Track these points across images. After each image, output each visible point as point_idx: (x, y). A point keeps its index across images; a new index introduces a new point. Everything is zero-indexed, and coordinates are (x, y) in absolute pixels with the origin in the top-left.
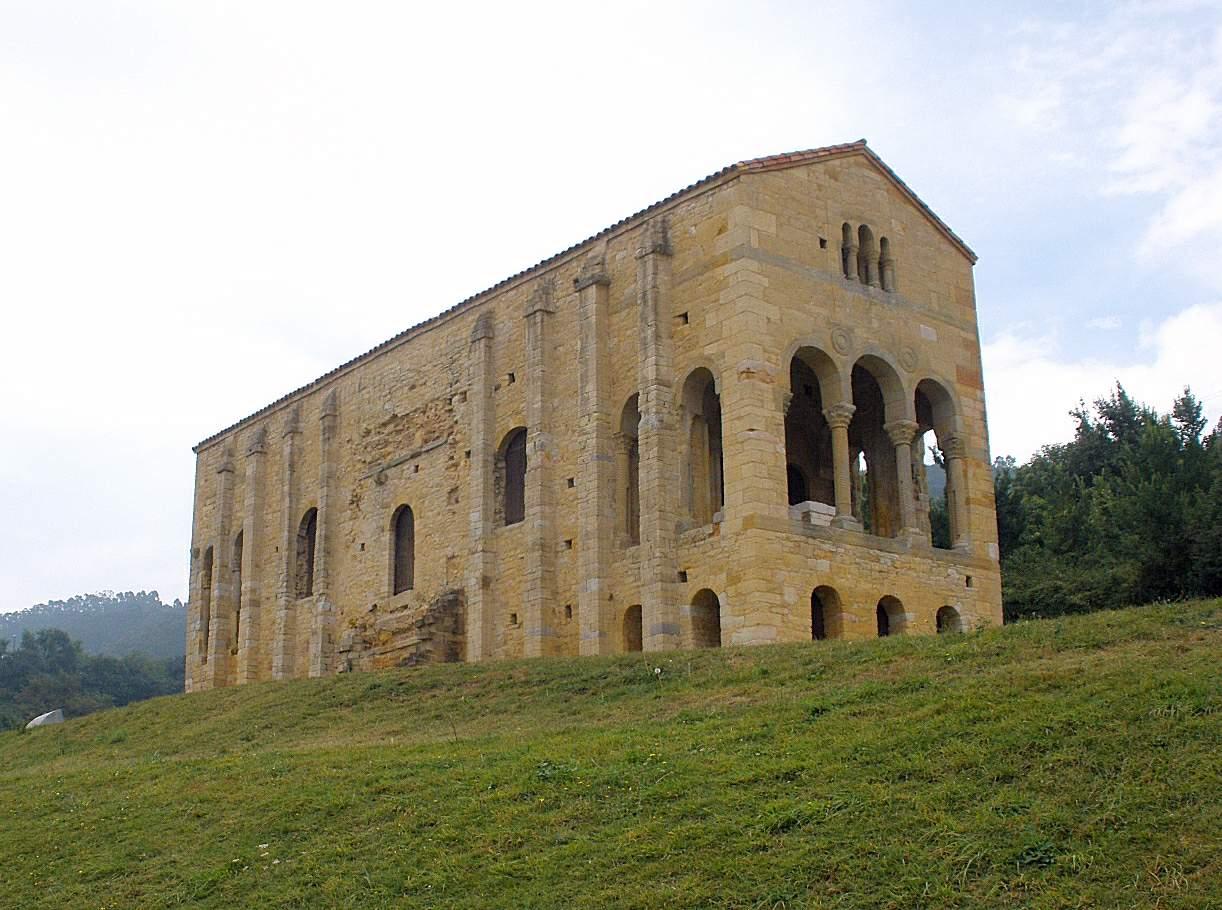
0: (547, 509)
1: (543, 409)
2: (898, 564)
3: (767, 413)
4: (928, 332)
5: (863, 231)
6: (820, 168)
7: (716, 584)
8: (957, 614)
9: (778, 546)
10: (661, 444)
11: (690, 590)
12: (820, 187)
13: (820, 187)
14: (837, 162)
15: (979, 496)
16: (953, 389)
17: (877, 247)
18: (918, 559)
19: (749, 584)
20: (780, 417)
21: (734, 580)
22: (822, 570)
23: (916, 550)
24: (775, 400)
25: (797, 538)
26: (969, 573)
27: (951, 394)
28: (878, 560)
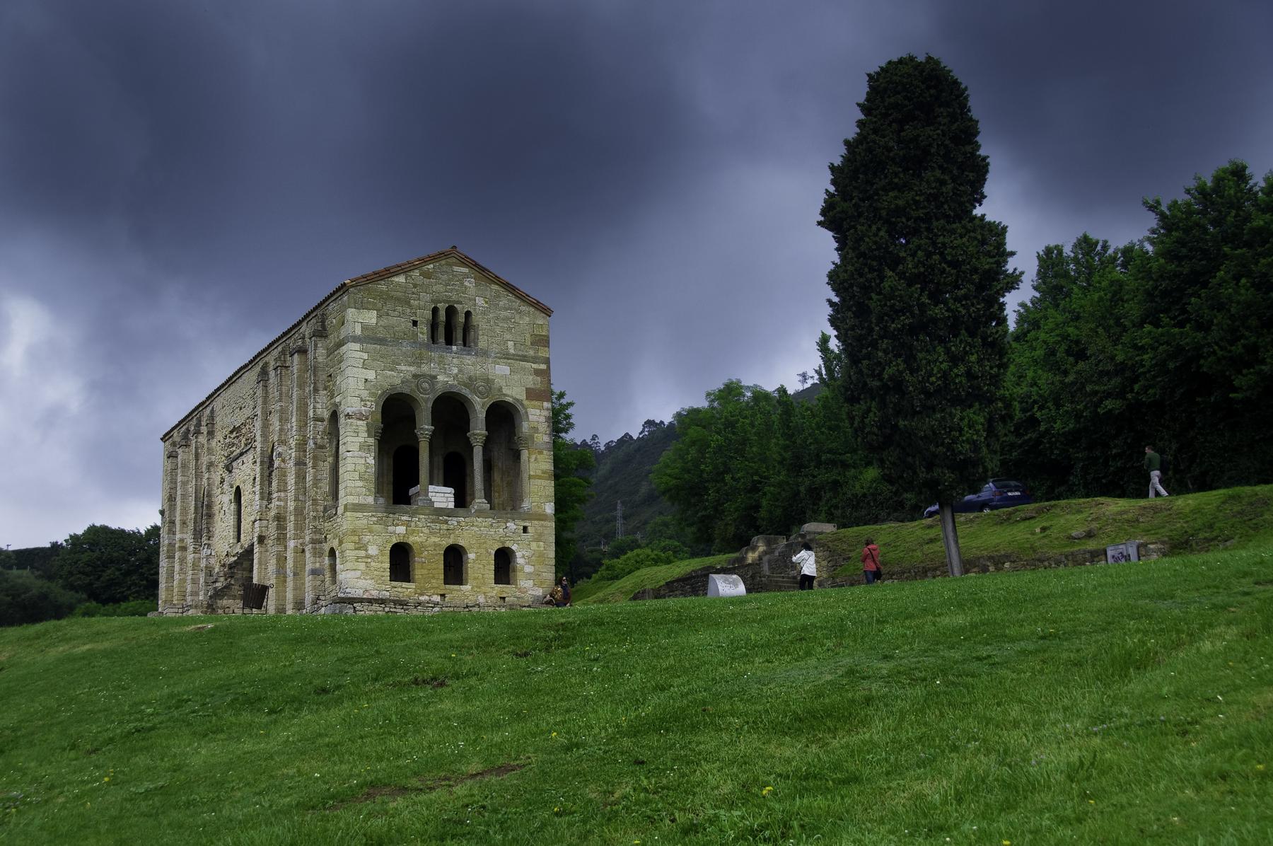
0: (282, 494)
1: (281, 430)
4: (500, 370)
5: (451, 311)
7: (335, 544)
8: (513, 552)
9: (365, 522)
10: (315, 458)
11: (327, 547)
16: (522, 405)
17: (462, 319)
19: (348, 545)
20: (371, 441)
21: (341, 543)
22: (399, 532)
23: (480, 513)
24: (368, 431)
26: (526, 524)
27: (520, 408)
28: (446, 522)
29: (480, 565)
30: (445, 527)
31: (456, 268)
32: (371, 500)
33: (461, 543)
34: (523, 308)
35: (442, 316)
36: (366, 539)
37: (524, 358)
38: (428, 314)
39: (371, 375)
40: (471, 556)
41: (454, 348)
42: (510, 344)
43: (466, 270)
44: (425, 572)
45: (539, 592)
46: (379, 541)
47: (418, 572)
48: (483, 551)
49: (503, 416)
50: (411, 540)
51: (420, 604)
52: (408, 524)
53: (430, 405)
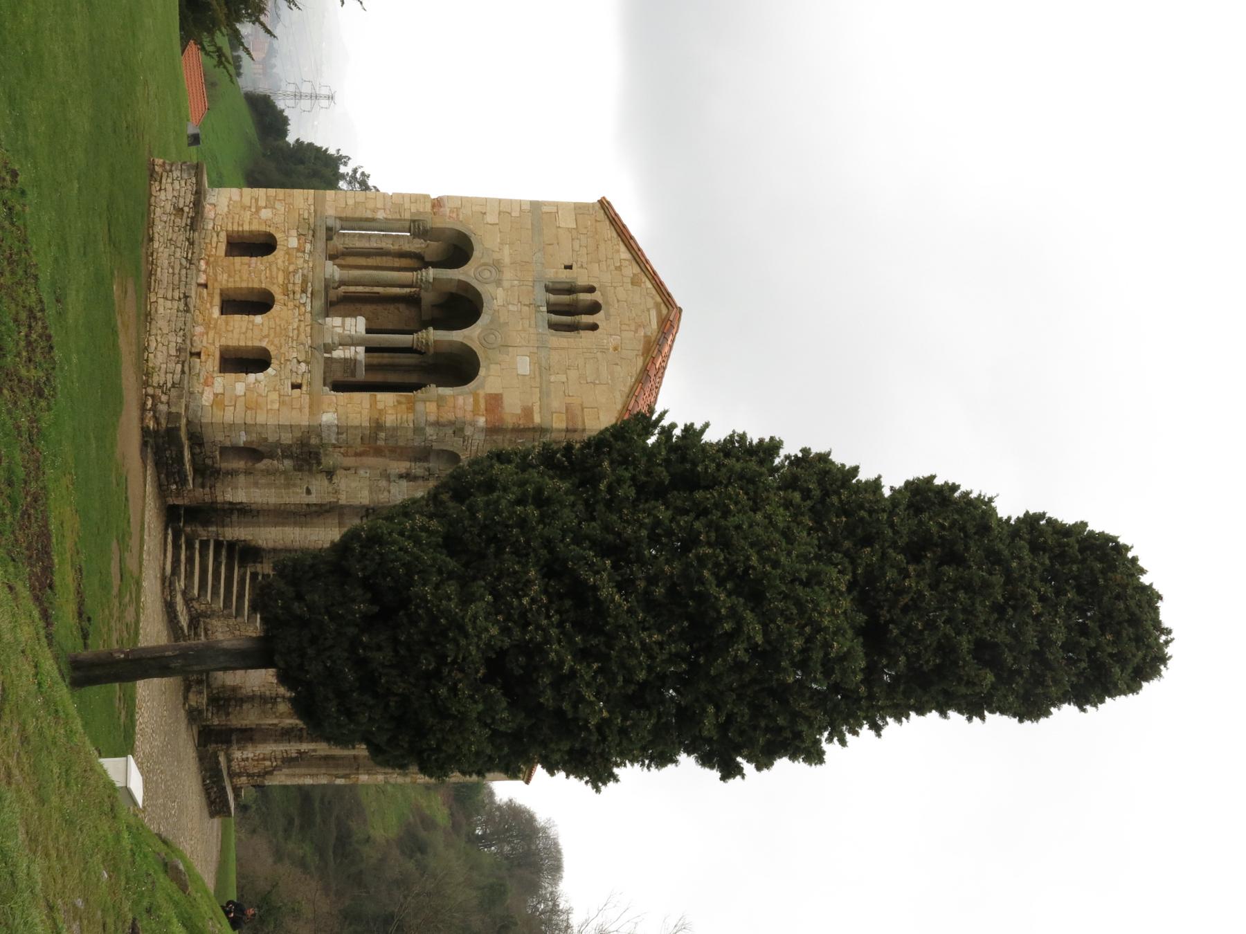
2: (303, 309)
3: (407, 206)
4: (524, 365)
6: (636, 270)
12: (619, 268)
13: (619, 268)
14: (649, 285)
15: (380, 406)
18: (308, 329)
20: (407, 216)
22: (289, 241)
23: (317, 329)
25: (312, 220)
26: (304, 388)
27: (472, 385)
28: (304, 291)
29: (245, 331)
30: (298, 289)
31: (653, 313)
32: (330, 212)
33: (276, 308)
34: (618, 395)
35: (584, 297)
36: (278, 205)
37: (544, 394)
38: (582, 281)
39: (492, 218)
40: (258, 319)
41: (545, 309)
42: (563, 378)
43: (654, 325)
44: (237, 267)
45: (207, 398)
46: (279, 220)
47: (241, 262)
48: (265, 332)
49: (459, 368)
50: (279, 253)
51: (192, 244)
52: (300, 249)
53: (462, 278)
